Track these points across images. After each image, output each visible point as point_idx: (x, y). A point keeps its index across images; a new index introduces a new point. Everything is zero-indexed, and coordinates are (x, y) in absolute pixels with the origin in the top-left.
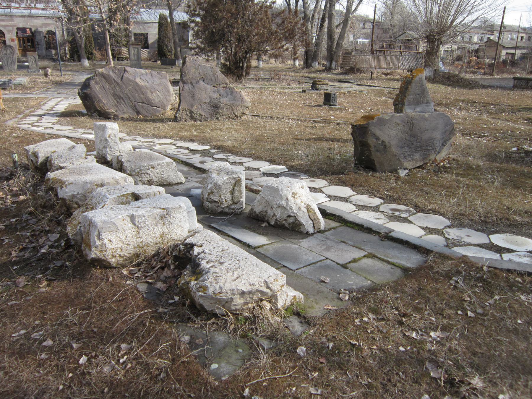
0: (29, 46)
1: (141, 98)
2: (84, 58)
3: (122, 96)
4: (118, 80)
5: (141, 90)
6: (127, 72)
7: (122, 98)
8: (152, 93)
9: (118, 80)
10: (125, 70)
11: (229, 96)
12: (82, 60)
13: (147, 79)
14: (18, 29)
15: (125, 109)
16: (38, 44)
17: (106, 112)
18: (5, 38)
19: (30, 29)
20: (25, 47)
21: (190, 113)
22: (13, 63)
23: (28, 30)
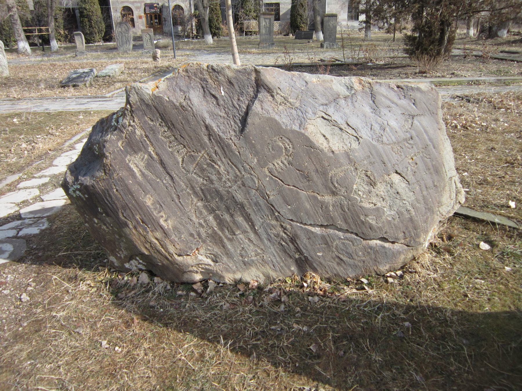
0: (156, 22)
1: (323, 206)
2: (207, 34)
3: (240, 197)
4: (227, 131)
5: (324, 174)
6: (269, 90)
7: (242, 207)
8: (372, 184)
9: (227, 131)
10: (260, 85)
12: (206, 36)
13: (354, 121)
14: (146, 5)
15: (251, 251)
16: (165, 21)
17: (173, 263)
18: (133, 15)
22: (128, 41)
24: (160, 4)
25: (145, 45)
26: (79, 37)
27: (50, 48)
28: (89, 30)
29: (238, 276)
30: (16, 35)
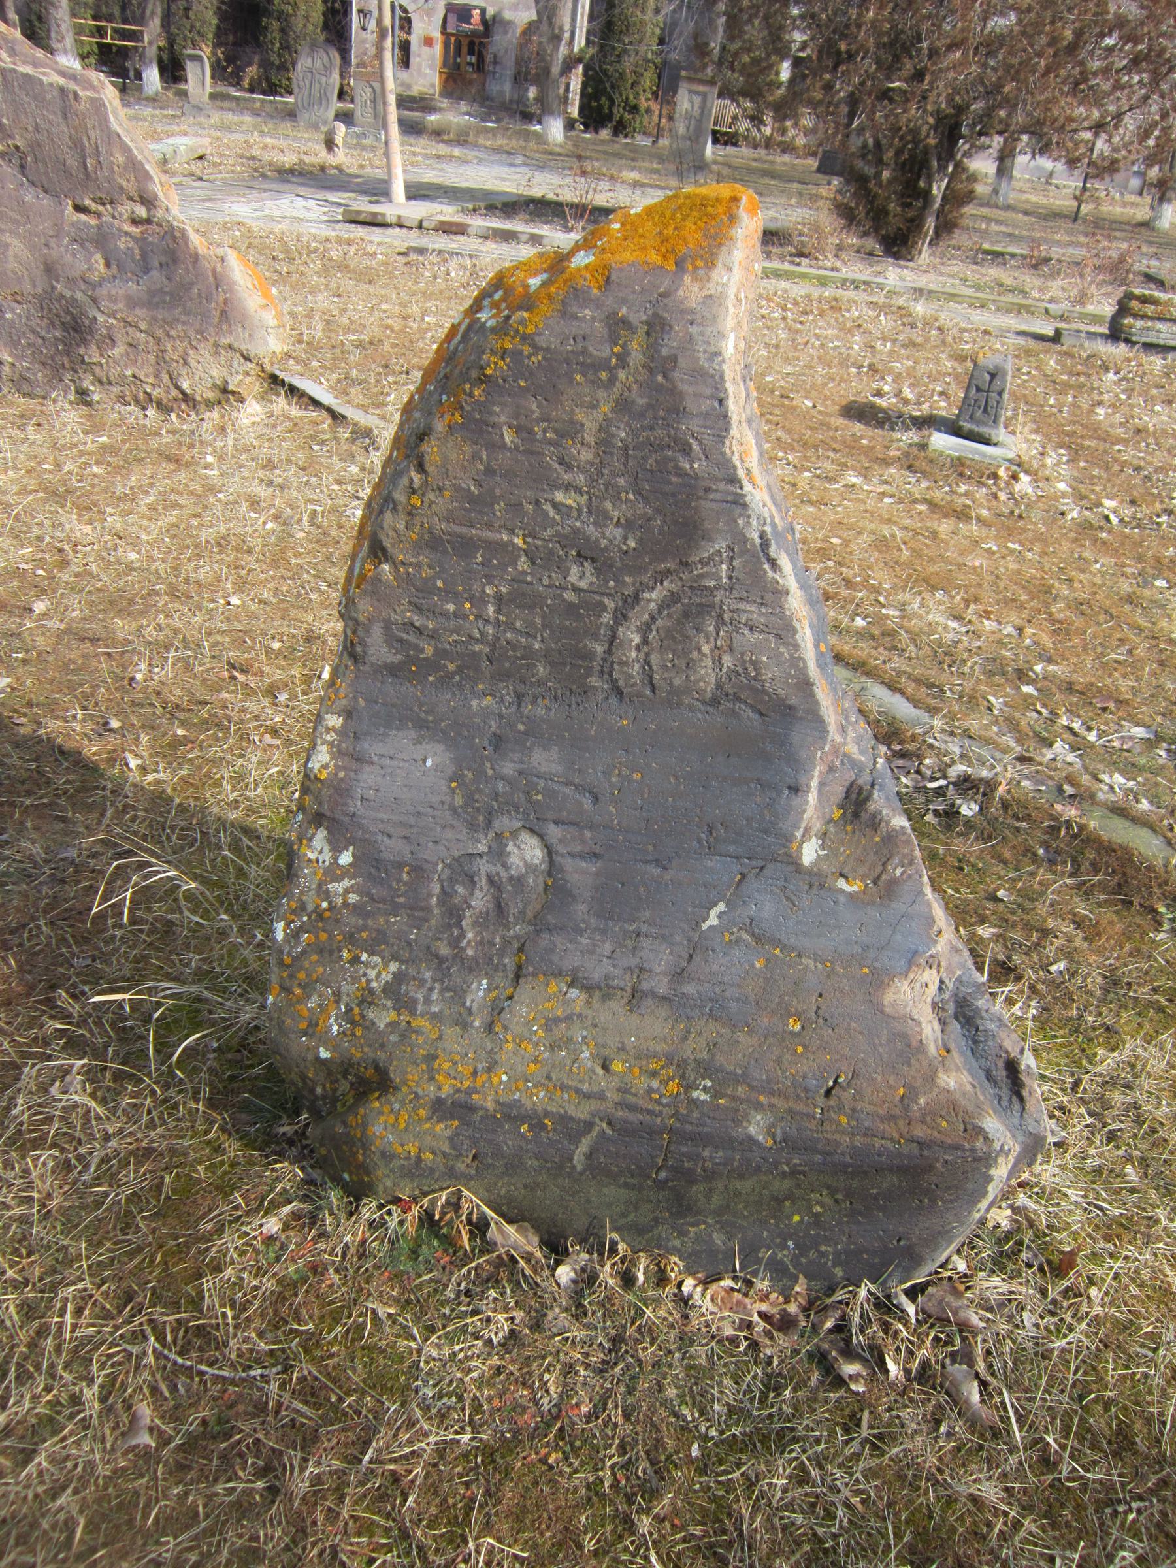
0: (470, 64)
11: (155, 274)
16: (495, 63)
18: (409, 33)
19: (483, 11)
20: (458, 66)
23: (476, 13)
24: (490, 12)
25: (358, 114)
26: (197, 64)
27: (140, 88)
28: (279, 56)
30: (53, 35)
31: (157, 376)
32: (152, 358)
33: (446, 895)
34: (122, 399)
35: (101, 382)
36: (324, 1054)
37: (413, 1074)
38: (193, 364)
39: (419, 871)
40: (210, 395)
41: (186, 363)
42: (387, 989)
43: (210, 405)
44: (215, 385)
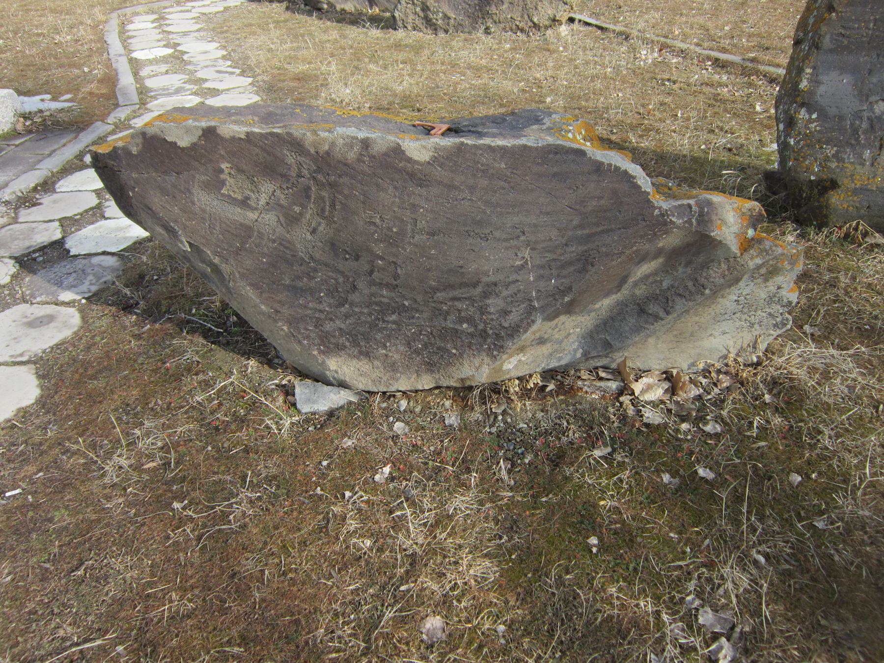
21: (423, 10)
29: (342, 6)
31: (522, 17)
32: (520, 8)
33: (852, 124)
34: (504, 29)
35: (495, 22)
36: (813, 178)
37: (846, 181)
38: (540, 9)
39: (841, 118)
40: (547, 23)
41: (536, 9)
42: (833, 156)
43: (546, 28)
44: (549, 18)
